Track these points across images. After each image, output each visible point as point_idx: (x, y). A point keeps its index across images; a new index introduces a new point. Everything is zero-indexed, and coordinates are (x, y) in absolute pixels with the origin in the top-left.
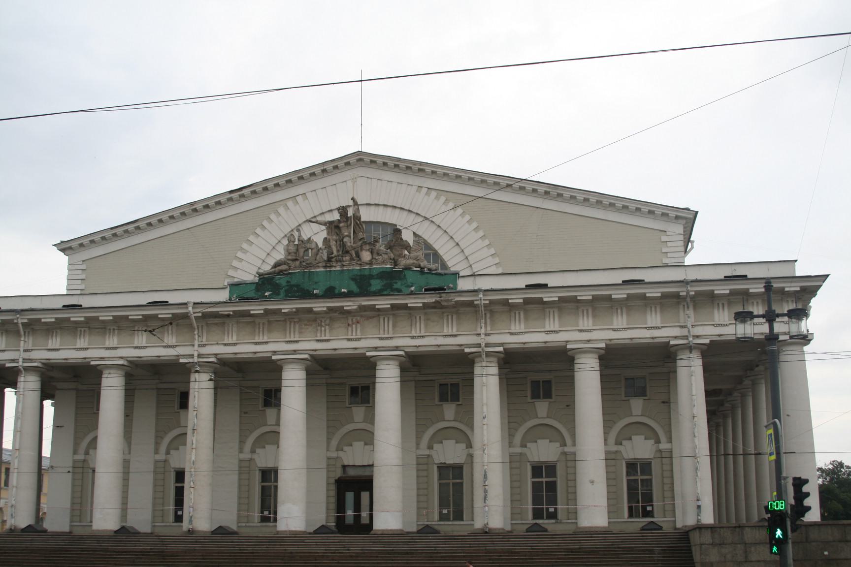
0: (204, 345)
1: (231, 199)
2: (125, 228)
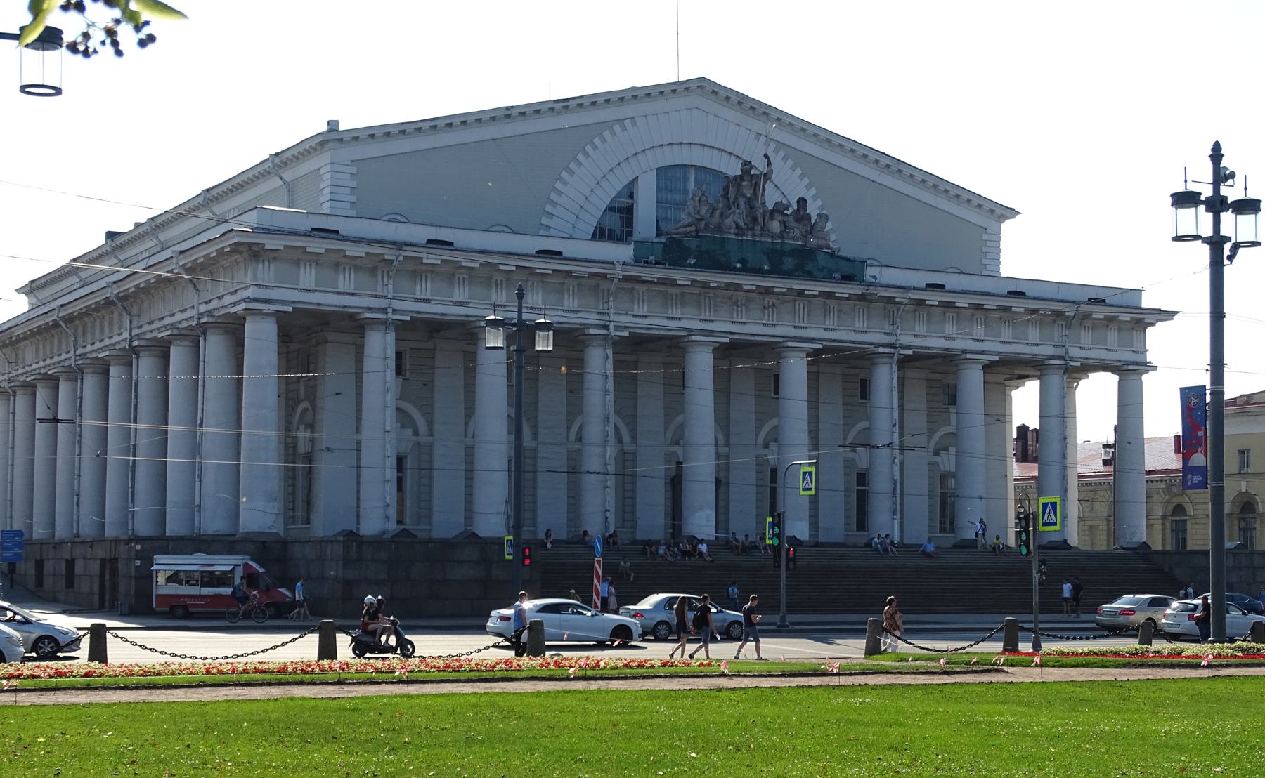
2: (420, 125)
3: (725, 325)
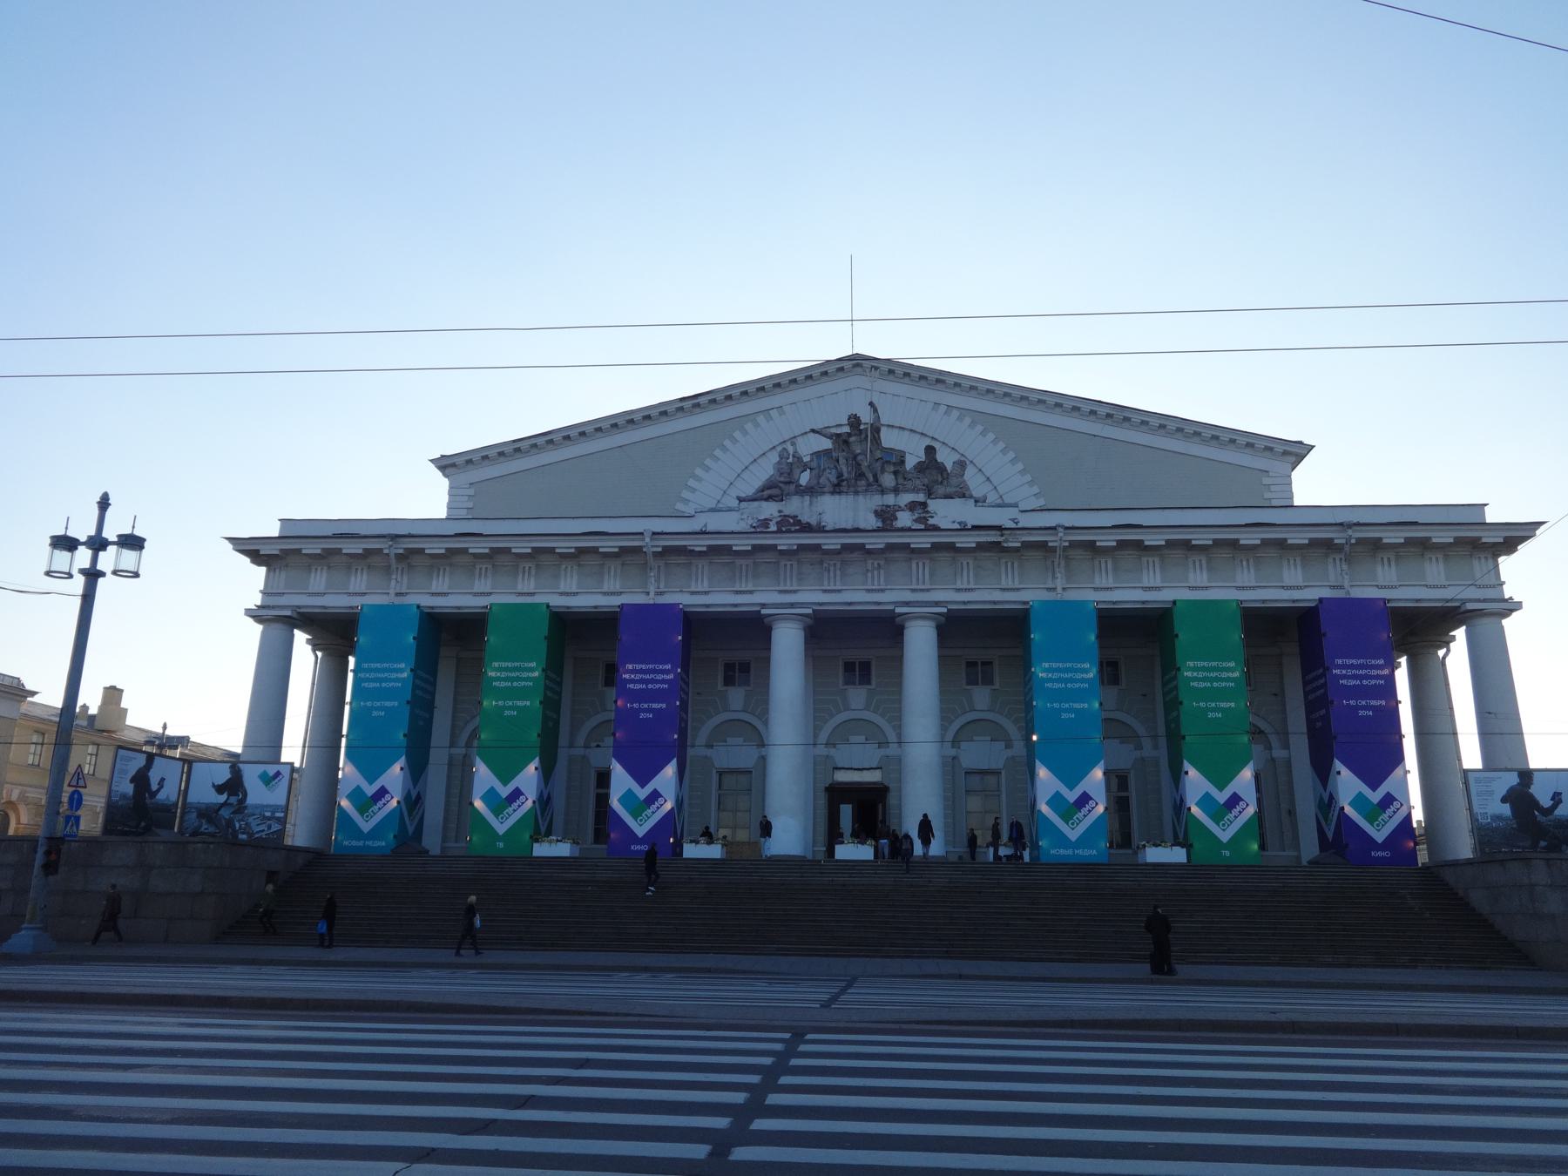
0: (662, 593)
1: (681, 409)
2: (533, 441)
3: (813, 596)
